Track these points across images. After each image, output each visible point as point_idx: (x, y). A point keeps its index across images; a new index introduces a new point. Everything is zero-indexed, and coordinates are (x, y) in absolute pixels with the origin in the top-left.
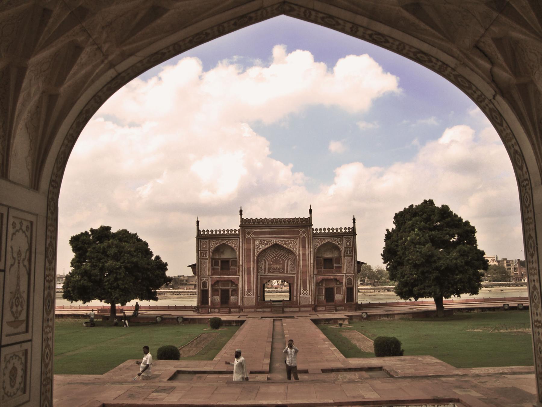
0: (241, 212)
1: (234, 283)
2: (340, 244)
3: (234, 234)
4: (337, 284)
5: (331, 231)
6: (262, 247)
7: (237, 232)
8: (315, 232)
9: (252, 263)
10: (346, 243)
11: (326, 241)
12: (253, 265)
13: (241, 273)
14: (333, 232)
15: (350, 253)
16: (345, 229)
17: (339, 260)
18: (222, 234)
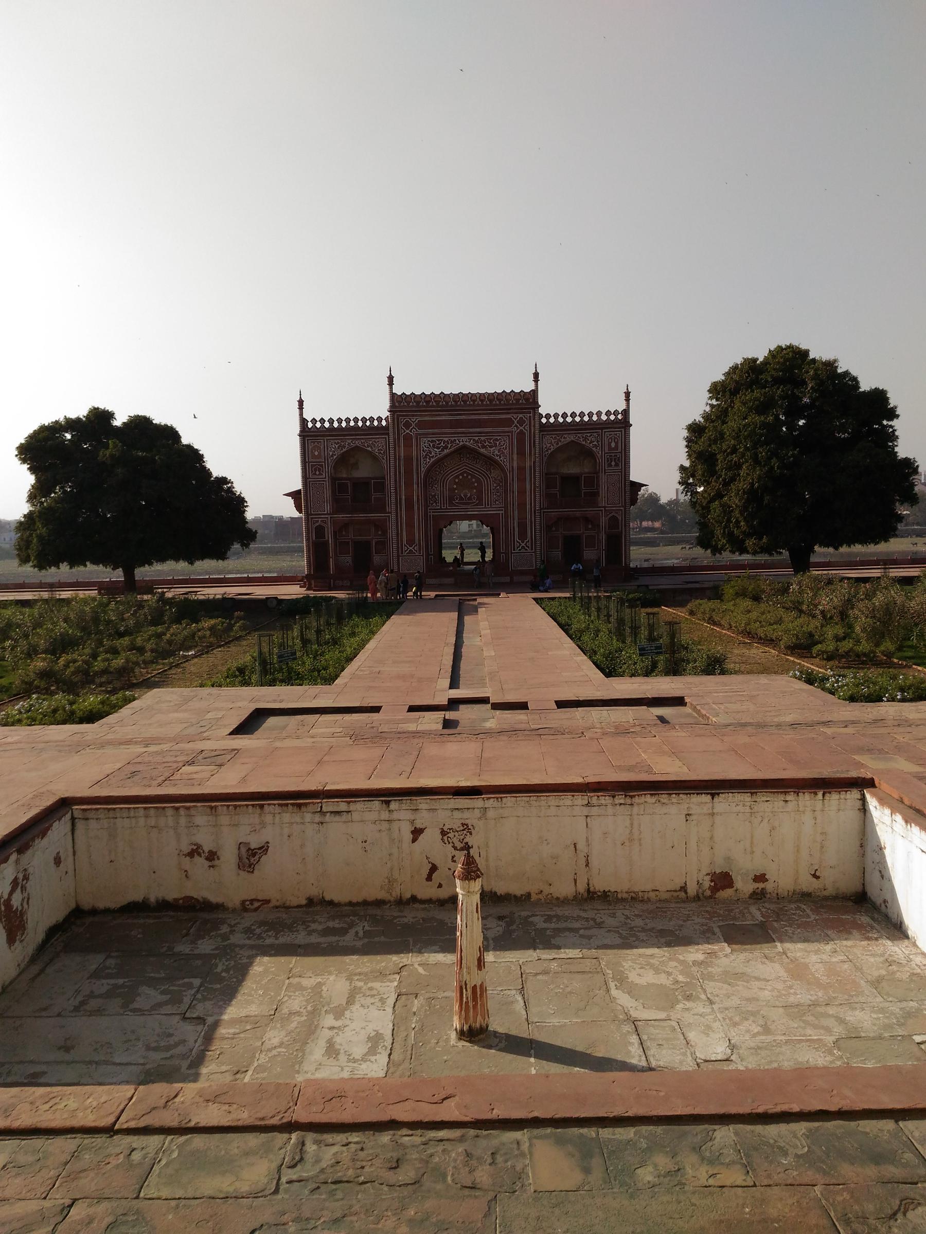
0: (391, 379)
1: (381, 526)
5: (578, 419)
8: (544, 420)
9: (415, 486)
10: (609, 444)
11: (568, 440)
13: (393, 507)
14: (582, 420)
15: (617, 465)
16: (608, 413)
17: (592, 480)
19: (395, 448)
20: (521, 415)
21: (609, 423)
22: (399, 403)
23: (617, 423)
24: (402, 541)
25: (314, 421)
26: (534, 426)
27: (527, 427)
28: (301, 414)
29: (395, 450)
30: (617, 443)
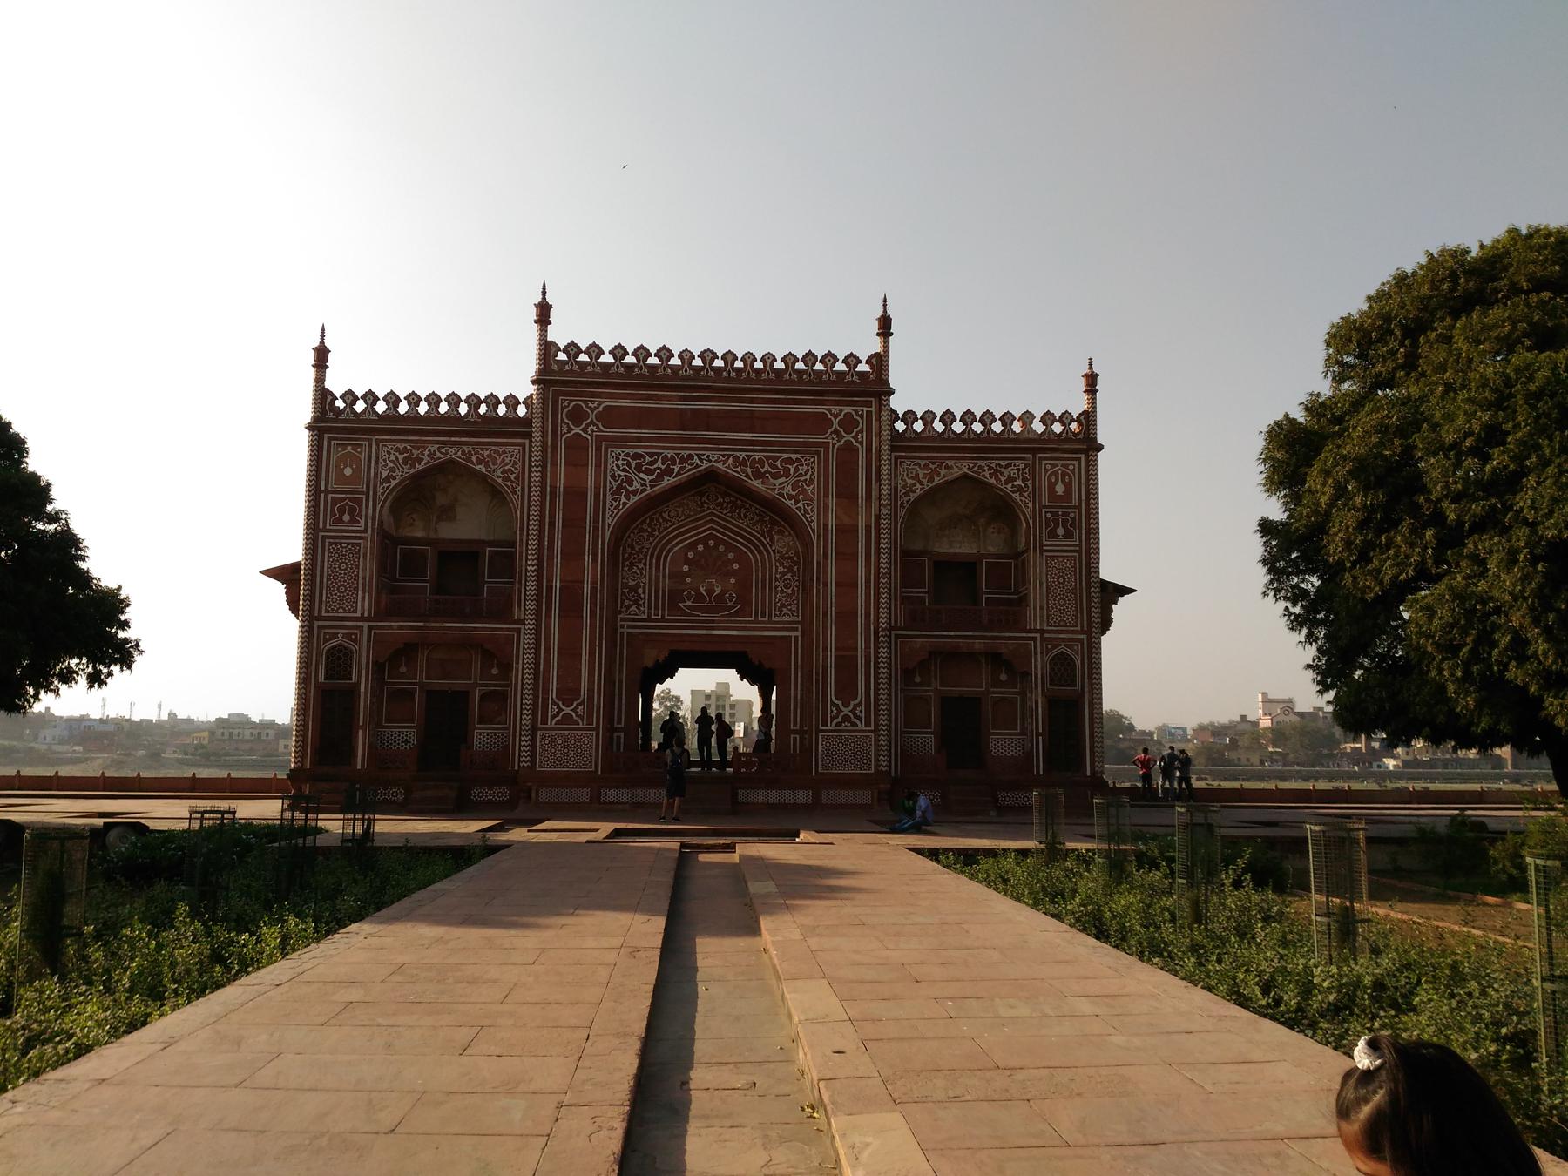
2: (1020, 490)
3: (504, 420)
4: (996, 683)
5: (978, 427)
6: (644, 485)
7: (522, 411)
8: (900, 426)
9: (588, 559)
10: (1052, 487)
11: (956, 472)
12: (590, 571)
13: (531, 606)
14: (988, 430)
15: (1068, 535)
16: (1048, 418)
17: (1010, 570)
18: (445, 417)
19: (544, 467)
20: (847, 409)
21: (1049, 440)
22: (562, 373)
23: (1068, 440)
24: (546, 691)
25: (350, 397)
26: (879, 435)
27: (863, 437)
28: (320, 380)
29: (544, 473)
30: (1068, 486)
